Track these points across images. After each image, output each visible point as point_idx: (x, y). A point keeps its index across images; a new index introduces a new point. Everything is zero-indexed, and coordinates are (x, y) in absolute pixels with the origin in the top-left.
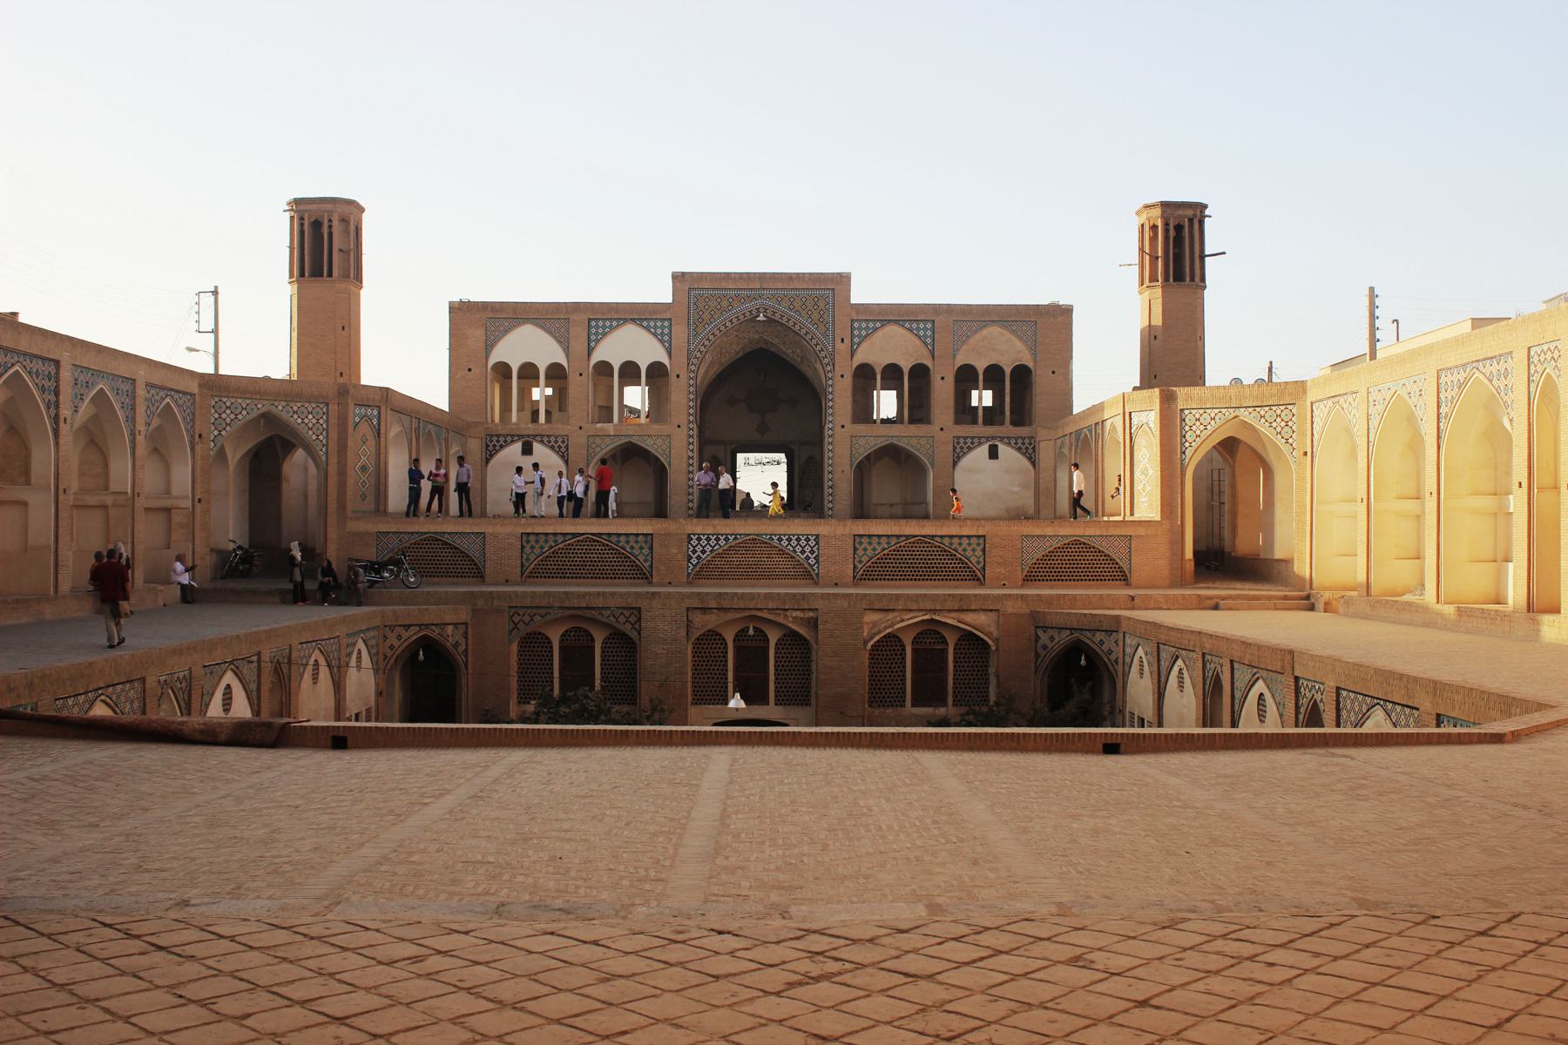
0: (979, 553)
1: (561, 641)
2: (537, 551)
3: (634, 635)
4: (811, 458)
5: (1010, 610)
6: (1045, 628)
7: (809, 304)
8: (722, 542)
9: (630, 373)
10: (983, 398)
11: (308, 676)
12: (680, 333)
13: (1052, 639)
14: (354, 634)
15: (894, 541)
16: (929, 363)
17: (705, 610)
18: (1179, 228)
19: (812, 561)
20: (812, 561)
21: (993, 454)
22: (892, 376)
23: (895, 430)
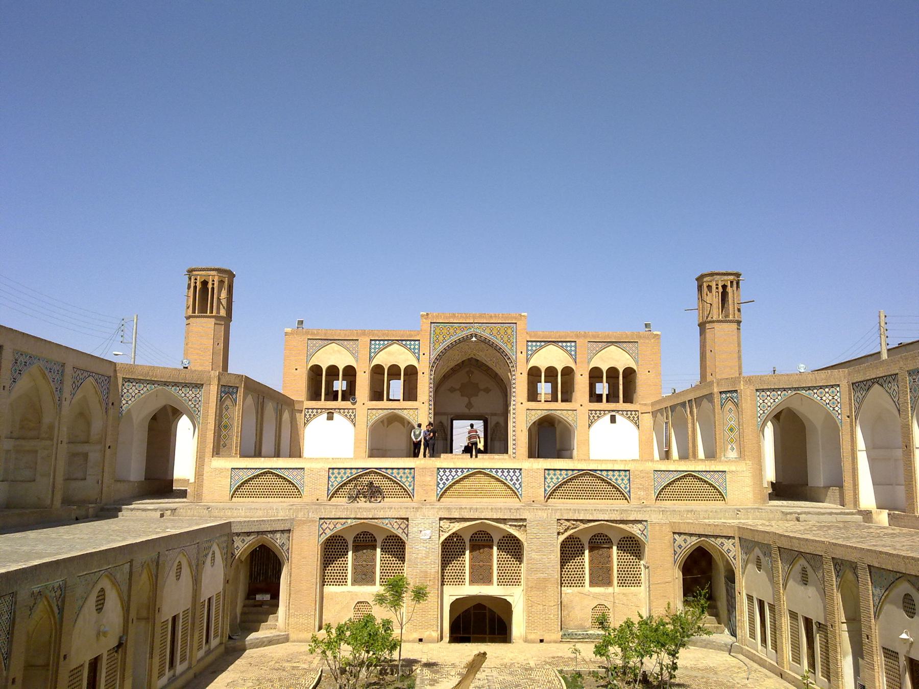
0: (626, 481)
1: (354, 541)
2: (339, 479)
3: (403, 537)
4: (498, 423)
5: (655, 521)
6: (680, 534)
7: (502, 332)
8: (460, 473)
9: (394, 372)
10: (602, 388)
11: (173, 574)
12: (425, 348)
13: (685, 541)
14: (210, 541)
15: (570, 473)
16: (573, 366)
17: (452, 520)
18: (724, 287)
19: (518, 486)
20: (518, 486)
21: (613, 420)
22: (551, 372)
23: (553, 405)
